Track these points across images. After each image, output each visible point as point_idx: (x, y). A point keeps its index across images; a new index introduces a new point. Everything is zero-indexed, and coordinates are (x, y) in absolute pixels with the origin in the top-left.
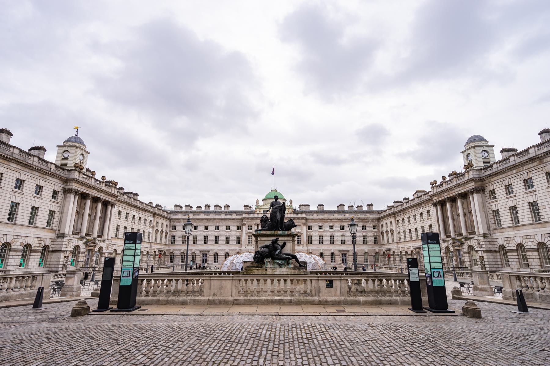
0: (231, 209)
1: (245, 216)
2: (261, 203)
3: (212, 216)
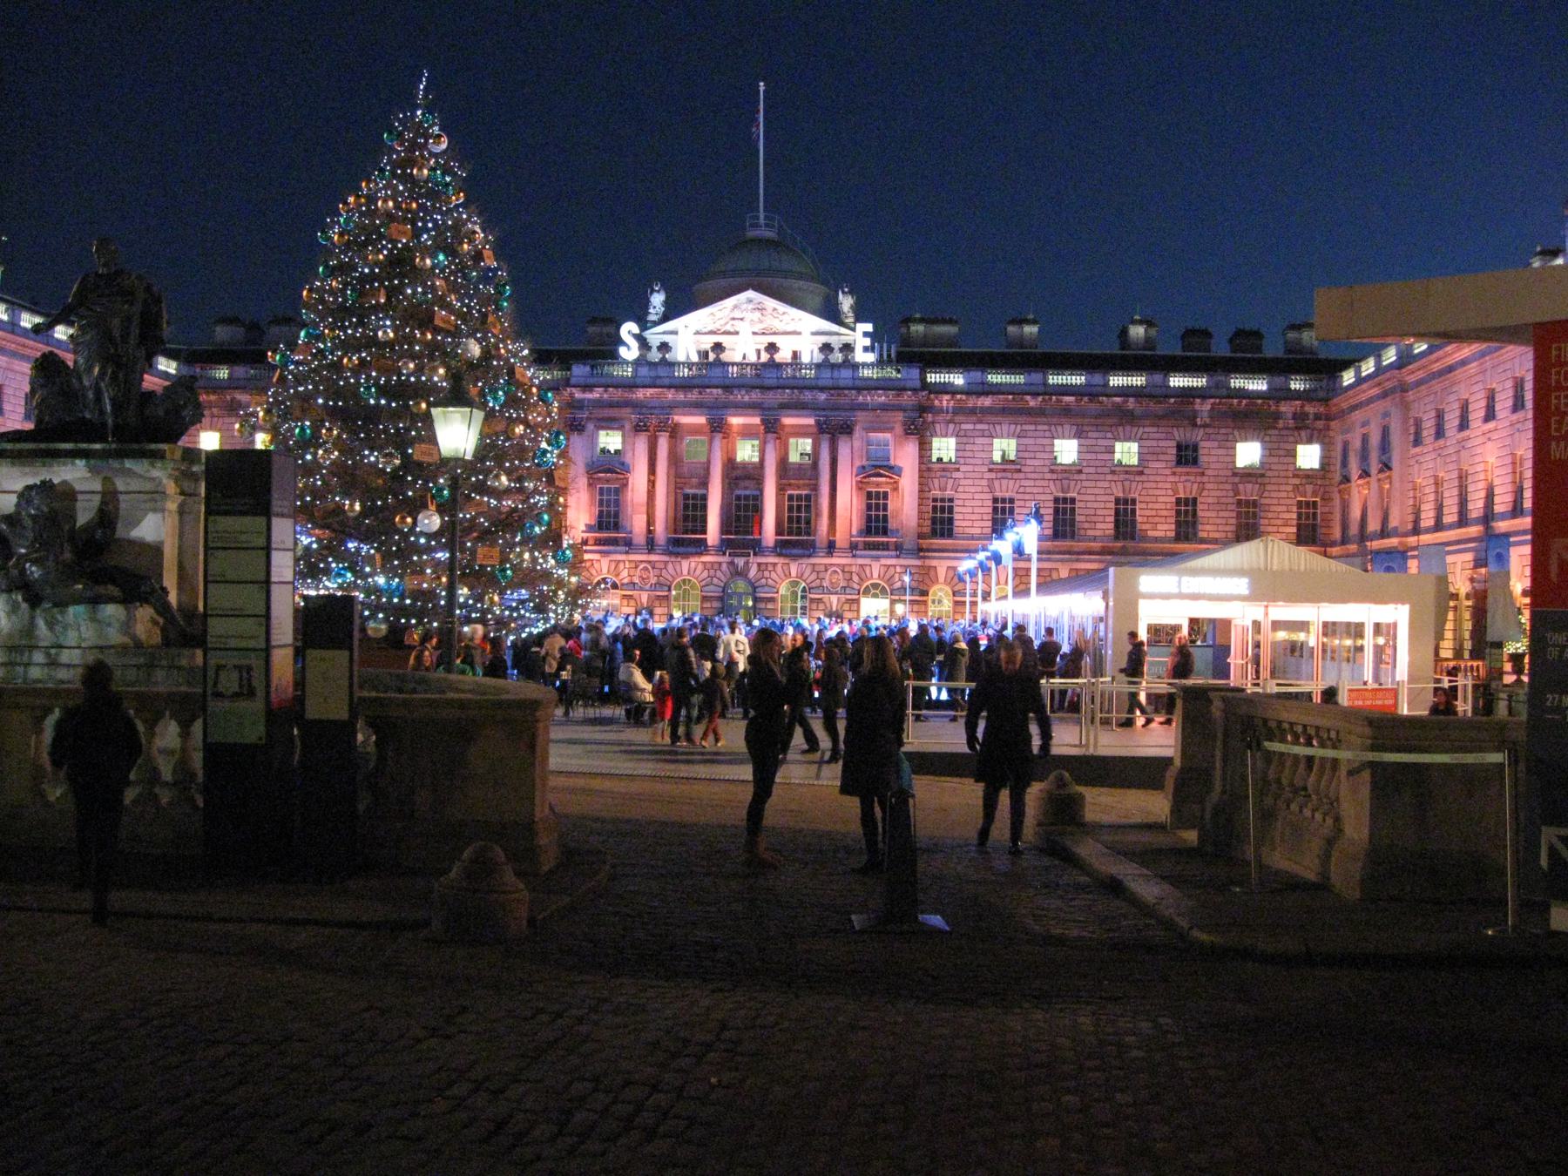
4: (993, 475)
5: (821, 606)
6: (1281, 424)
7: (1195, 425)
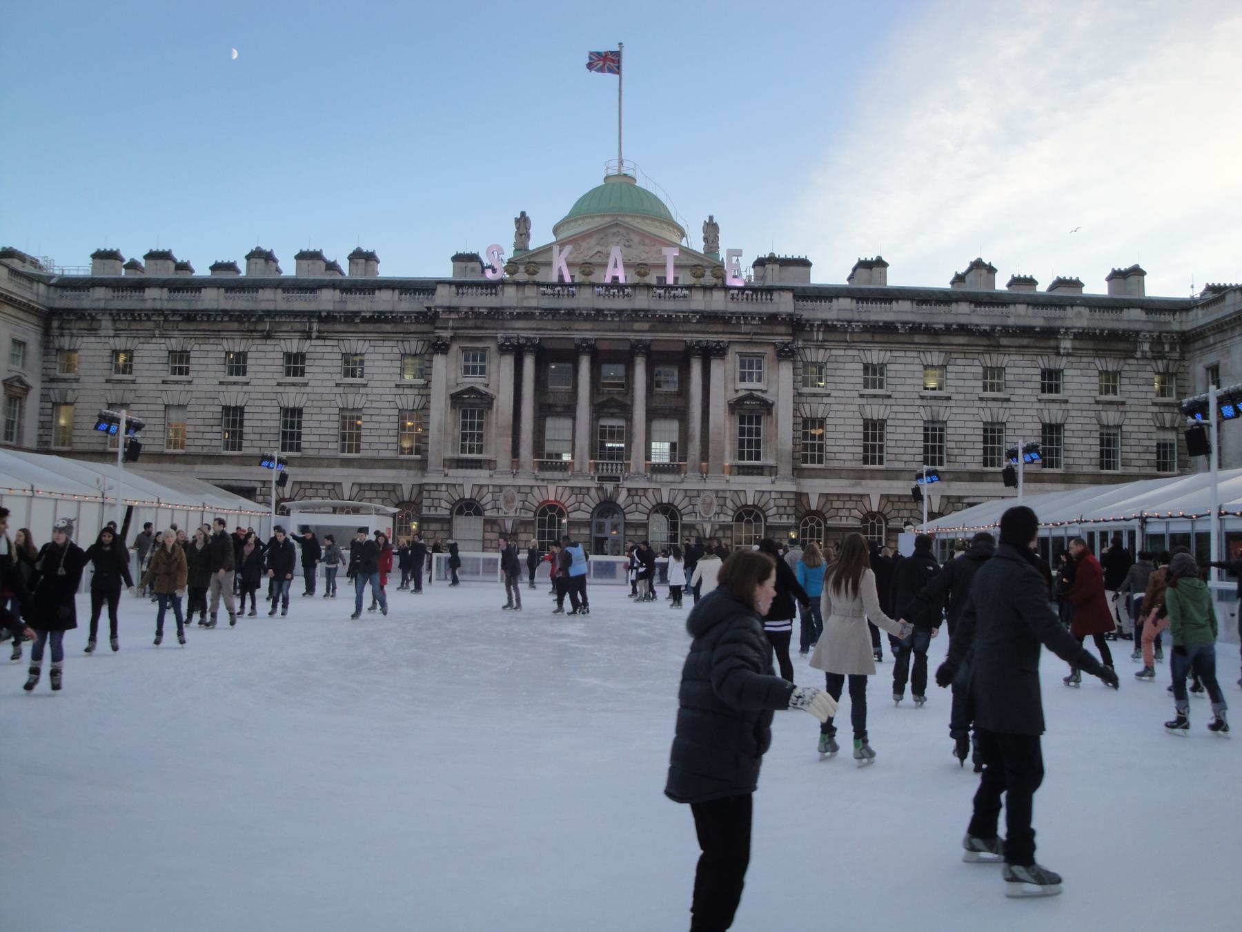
0: (385, 271)
1: (444, 297)
2: (540, 237)
3: (268, 300)
4: (864, 401)
5: (694, 533)
6: (1139, 354)
7: (1058, 354)
